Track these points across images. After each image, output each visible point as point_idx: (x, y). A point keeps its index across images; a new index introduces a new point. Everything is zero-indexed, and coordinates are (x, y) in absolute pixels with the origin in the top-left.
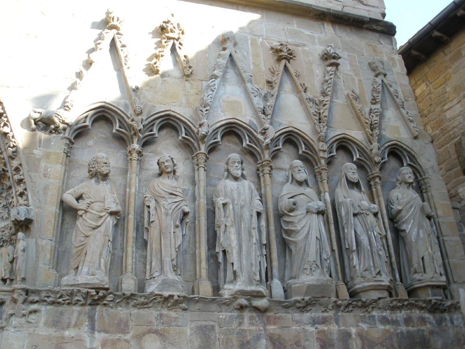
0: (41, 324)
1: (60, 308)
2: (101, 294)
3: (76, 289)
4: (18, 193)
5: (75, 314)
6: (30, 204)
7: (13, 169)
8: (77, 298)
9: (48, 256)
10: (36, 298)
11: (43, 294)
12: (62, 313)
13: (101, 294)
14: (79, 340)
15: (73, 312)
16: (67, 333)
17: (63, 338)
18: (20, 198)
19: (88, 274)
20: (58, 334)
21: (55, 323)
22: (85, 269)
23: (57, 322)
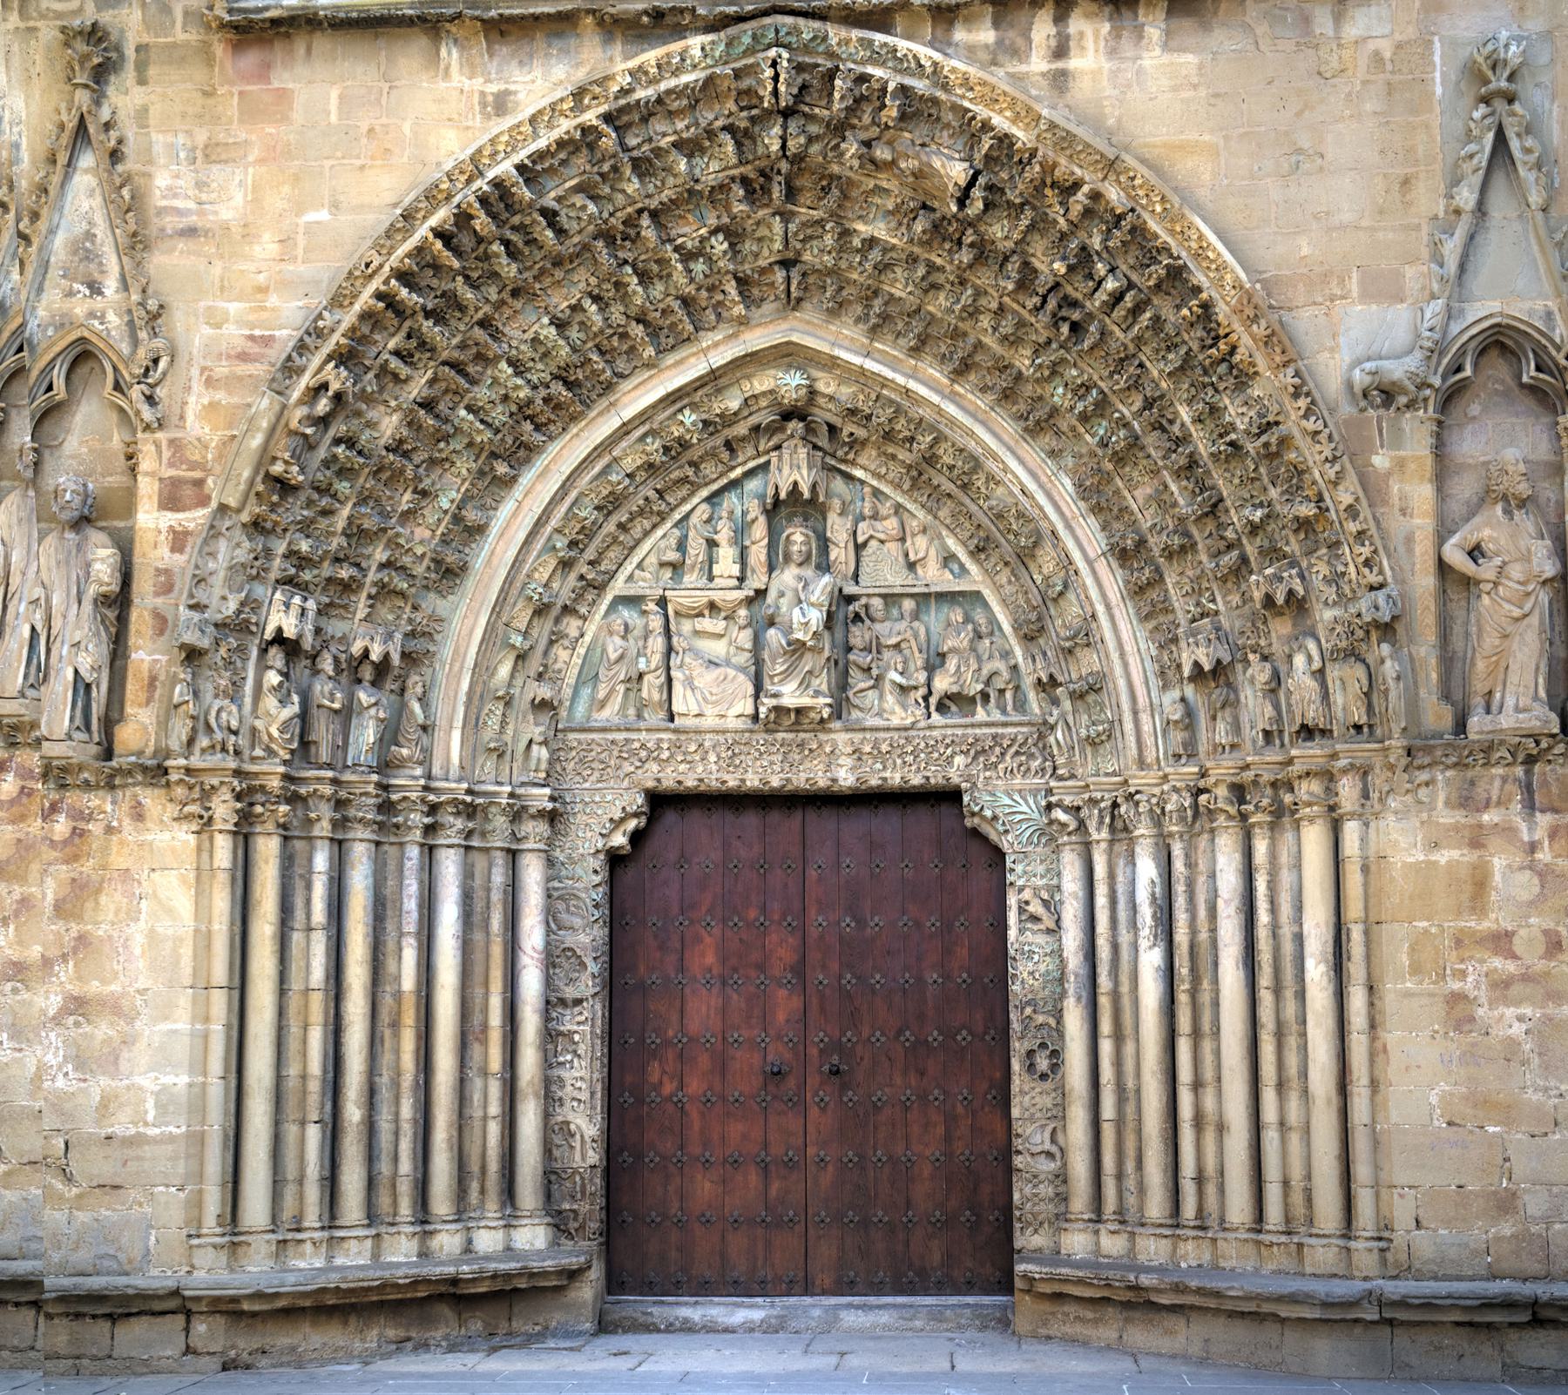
0: (1440, 804)
1: (1470, 774)
2: (1544, 745)
3: (1497, 738)
4: (1362, 559)
5: (1497, 783)
6: (1390, 580)
7: (1342, 507)
8: (1499, 754)
9: (1434, 676)
10: (1427, 760)
11: (1439, 753)
12: (1472, 783)
13: (1544, 745)
14: (1508, 831)
15: (1493, 778)
16: (1486, 817)
17: (1480, 826)
18: (1366, 571)
19: (1517, 710)
20: (1471, 821)
21: (1466, 800)
22: (1510, 702)
23: (1467, 799)
